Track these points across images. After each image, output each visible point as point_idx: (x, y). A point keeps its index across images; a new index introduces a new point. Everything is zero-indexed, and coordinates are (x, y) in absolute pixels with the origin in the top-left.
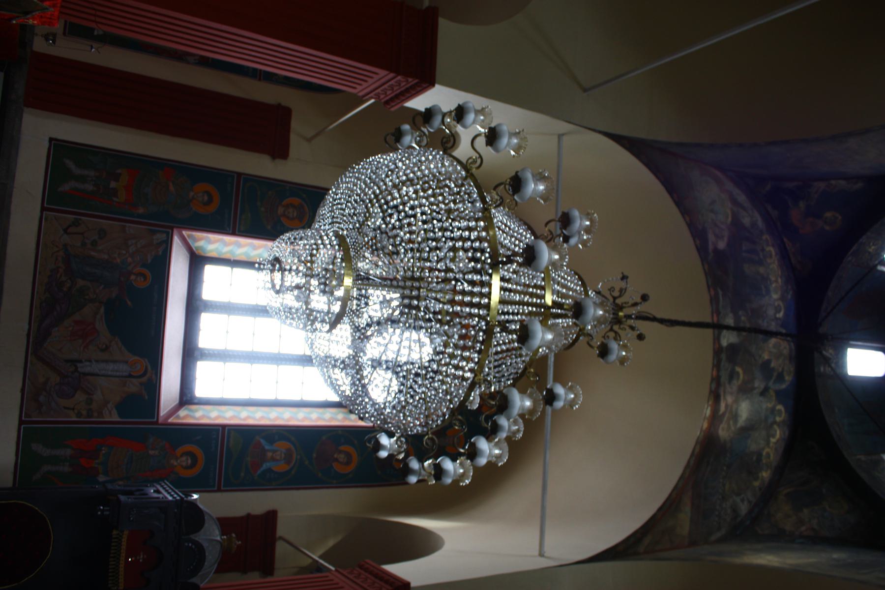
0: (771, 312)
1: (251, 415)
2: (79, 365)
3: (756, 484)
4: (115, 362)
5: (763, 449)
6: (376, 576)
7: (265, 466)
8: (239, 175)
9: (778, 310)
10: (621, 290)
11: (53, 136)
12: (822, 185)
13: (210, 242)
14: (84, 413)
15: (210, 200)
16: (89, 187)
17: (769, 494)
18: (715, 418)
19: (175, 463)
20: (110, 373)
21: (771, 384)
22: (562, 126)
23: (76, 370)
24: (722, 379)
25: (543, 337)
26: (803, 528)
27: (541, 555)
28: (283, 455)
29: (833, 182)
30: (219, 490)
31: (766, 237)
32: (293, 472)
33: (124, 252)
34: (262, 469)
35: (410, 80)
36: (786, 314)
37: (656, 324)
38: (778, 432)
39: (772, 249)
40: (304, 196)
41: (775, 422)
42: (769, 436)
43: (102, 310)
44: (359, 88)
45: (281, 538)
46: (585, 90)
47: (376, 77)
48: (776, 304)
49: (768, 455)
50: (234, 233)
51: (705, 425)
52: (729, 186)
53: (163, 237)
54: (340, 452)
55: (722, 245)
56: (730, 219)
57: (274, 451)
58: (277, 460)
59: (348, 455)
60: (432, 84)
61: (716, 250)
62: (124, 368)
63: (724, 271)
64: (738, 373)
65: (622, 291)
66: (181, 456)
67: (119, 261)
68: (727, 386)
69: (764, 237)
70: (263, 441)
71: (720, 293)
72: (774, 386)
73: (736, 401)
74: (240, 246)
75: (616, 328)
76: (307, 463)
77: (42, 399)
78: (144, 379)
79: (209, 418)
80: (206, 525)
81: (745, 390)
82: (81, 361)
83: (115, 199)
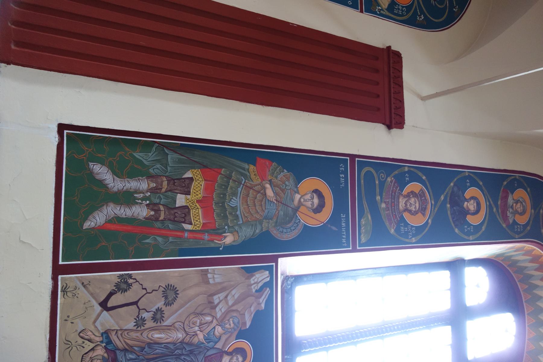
8: (353, 157)
11: (66, 121)
16: (141, 212)
33: (209, 318)
83: (187, 227)
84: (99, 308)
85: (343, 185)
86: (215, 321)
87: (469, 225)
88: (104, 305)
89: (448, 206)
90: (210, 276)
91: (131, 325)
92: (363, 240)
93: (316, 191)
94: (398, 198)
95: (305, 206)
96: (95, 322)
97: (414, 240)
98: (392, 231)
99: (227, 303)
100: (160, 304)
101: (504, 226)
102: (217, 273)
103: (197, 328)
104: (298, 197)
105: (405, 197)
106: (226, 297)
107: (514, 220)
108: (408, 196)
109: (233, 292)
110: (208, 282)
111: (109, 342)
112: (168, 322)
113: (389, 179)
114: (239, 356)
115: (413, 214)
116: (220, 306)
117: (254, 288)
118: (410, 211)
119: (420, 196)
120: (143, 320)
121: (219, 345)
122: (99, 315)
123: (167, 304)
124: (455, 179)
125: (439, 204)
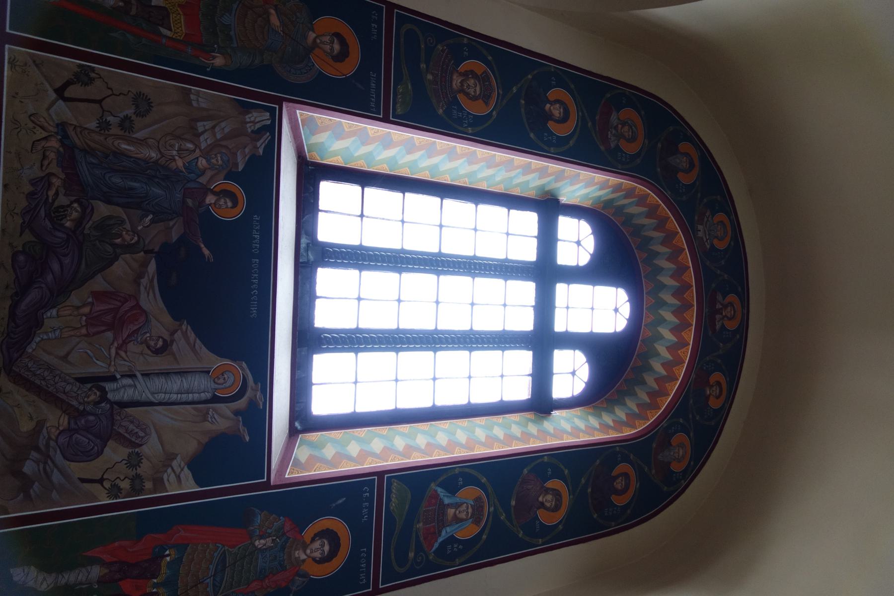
2: (108, 386)
4: (182, 373)
7: (444, 535)
13: (340, 135)
14: (125, 485)
19: (303, 557)
20: (174, 397)
23: (104, 398)
28: (470, 510)
32: (484, 537)
33: (190, 146)
40: (490, 58)
43: (152, 267)
50: (386, 120)
53: (264, 118)
54: (547, 491)
57: (457, 506)
58: (462, 520)
59: (557, 494)
62: (200, 385)
66: (313, 540)
67: (180, 163)
70: (439, 490)
74: (388, 144)
77: (29, 468)
78: (242, 403)
82: (113, 379)
84: (54, 96)
85: (375, 37)
86: (198, 151)
87: (551, 133)
88: (60, 92)
89: (523, 102)
90: (192, 97)
91: (93, 125)
92: (399, 111)
93: (337, 35)
95: (320, 48)
96: (48, 109)
97: (470, 130)
98: (440, 111)
99: (214, 135)
100: (130, 112)
101: (602, 148)
102: (203, 97)
103: (175, 153)
104: (312, 35)
105: (461, 74)
106: (213, 127)
107: (617, 146)
108: (466, 75)
109: (223, 124)
110: (190, 103)
111: (66, 136)
112: (139, 135)
113: (440, 47)
114: (228, 200)
115: (470, 99)
116: (205, 136)
117: (250, 128)
118: (467, 94)
119: (483, 79)
120: (108, 124)
121: (203, 180)
122: (53, 103)
123: (138, 114)
124: (535, 72)
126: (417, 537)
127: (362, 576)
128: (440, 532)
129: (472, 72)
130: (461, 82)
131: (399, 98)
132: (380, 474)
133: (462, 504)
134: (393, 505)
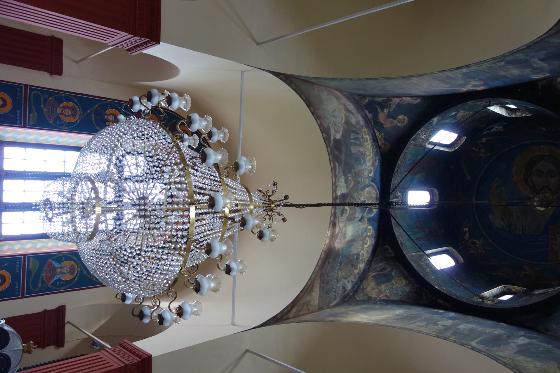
0: (366, 173)
1: (45, 245)
3: (356, 271)
5: (360, 251)
6: (130, 351)
7: (56, 278)
8: (26, 86)
9: (370, 172)
10: (273, 191)
12: (397, 100)
13: (7, 132)
15: (5, 104)
17: (363, 277)
18: (333, 236)
21: (365, 214)
22: (244, 67)
24: (337, 214)
25: (221, 249)
26: (381, 296)
27: (233, 324)
28: (68, 270)
29: (404, 98)
30: (23, 297)
31: (365, 129)
32: (76, 280)
34: (54, 280)
35: (143, 39)
36: (375, 174)
37: (293, 207)
38: (369, 241)
39: (367, 136)
40: (76, 100)
41: (367, 236)
42: (363, 244)
44: (108, 41)
45: (68, 322)
46: (258, 44)
47: (119, 36)
48: (369, 168)
49: (363, 254)
50: (25, 127)
51: (327, 241)
52: (344, 100)
55: (338, 136)
56: (344, 121)
57: (62, 268)
58: (64, 273)
60: (158, 42)
61: (335, 140)
63: (339, 153)
64: (346, 210)
65: (273, 192)
68: (340, 218)
69: (363, 130)
70: (53, 262)
71: (337, 164)
72: (367, 216)
73: (345, 226)
74: (30, 134)
75: (270, 213)
76: (85, 273)
79: (14, 250)
80: (11, 341)
81: (350, 219)
89: (93, 116)
92: (31, 123)
94: (57, 108)
97: (66, 128)
98: (51, 122)
105: (61, 108)
108: (64, 107)
113: (50, 98)
118: (64, 115)
119: (73, 109)
125: (86, 114)
126: (42, 279)
127: (17, 292)
128: (53, 277)
129: (67, 106)
130: (62, 111)
131: (31, 119)
132: (24, 255)
133: (64, 267)
134: (30, 267)
